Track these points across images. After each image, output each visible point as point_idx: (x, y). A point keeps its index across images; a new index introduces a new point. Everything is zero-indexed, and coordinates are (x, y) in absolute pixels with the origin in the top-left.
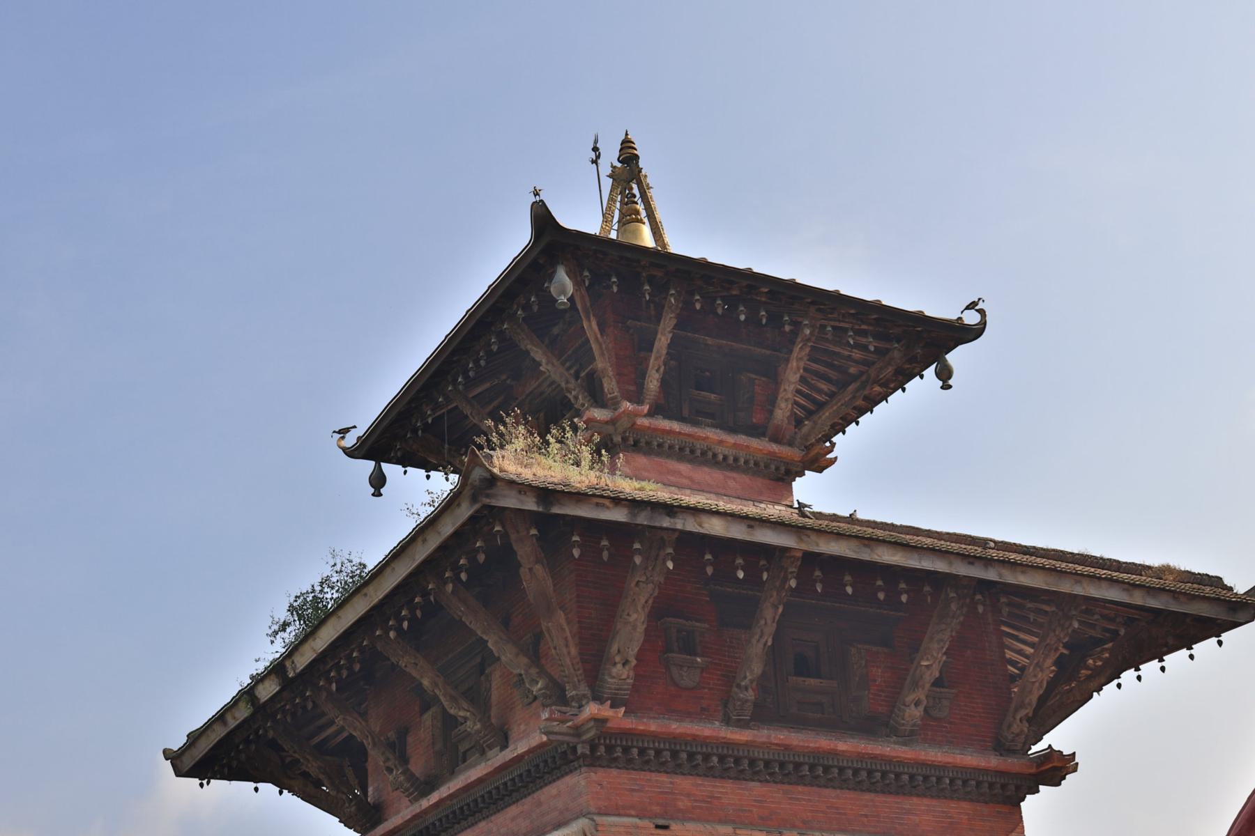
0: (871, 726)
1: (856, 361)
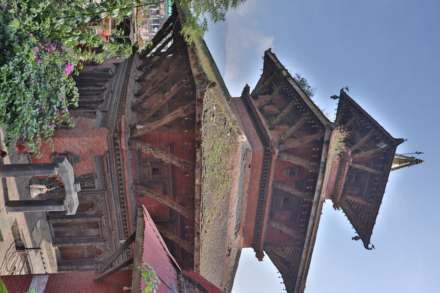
0: (271, 215)
1: (361, 216)
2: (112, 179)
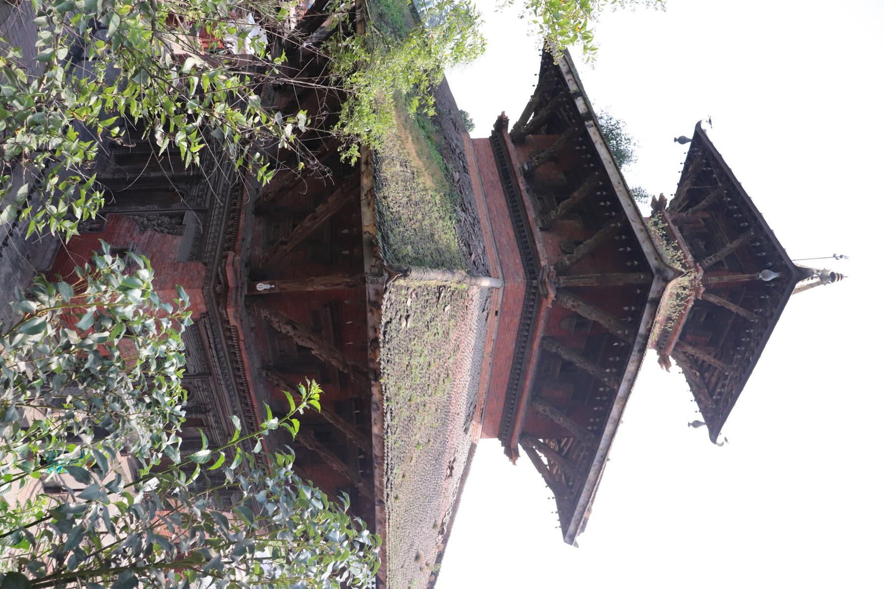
2: (218, 359)
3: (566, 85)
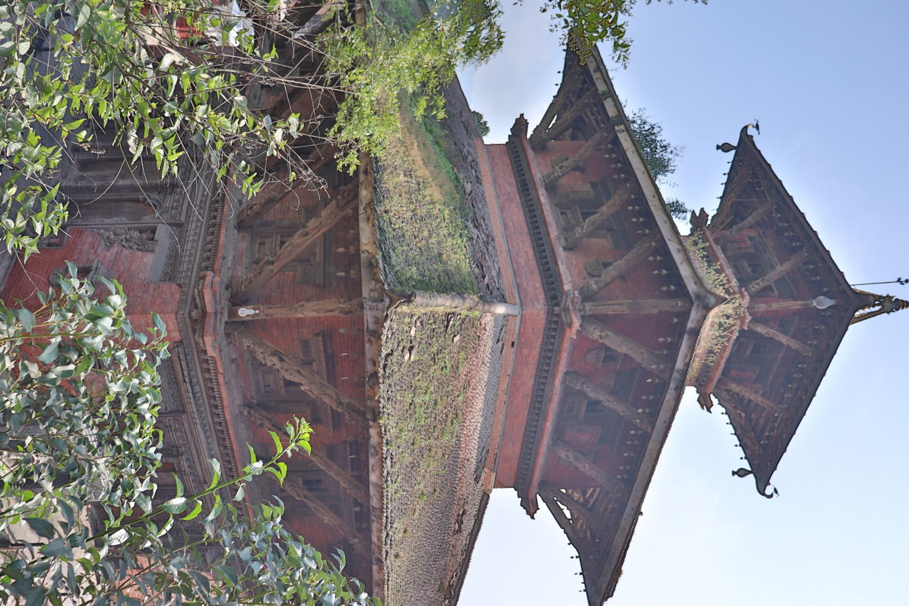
0: (558, 432)
1: (757, 420)
2: (194, 394)
3: (594, 84)
